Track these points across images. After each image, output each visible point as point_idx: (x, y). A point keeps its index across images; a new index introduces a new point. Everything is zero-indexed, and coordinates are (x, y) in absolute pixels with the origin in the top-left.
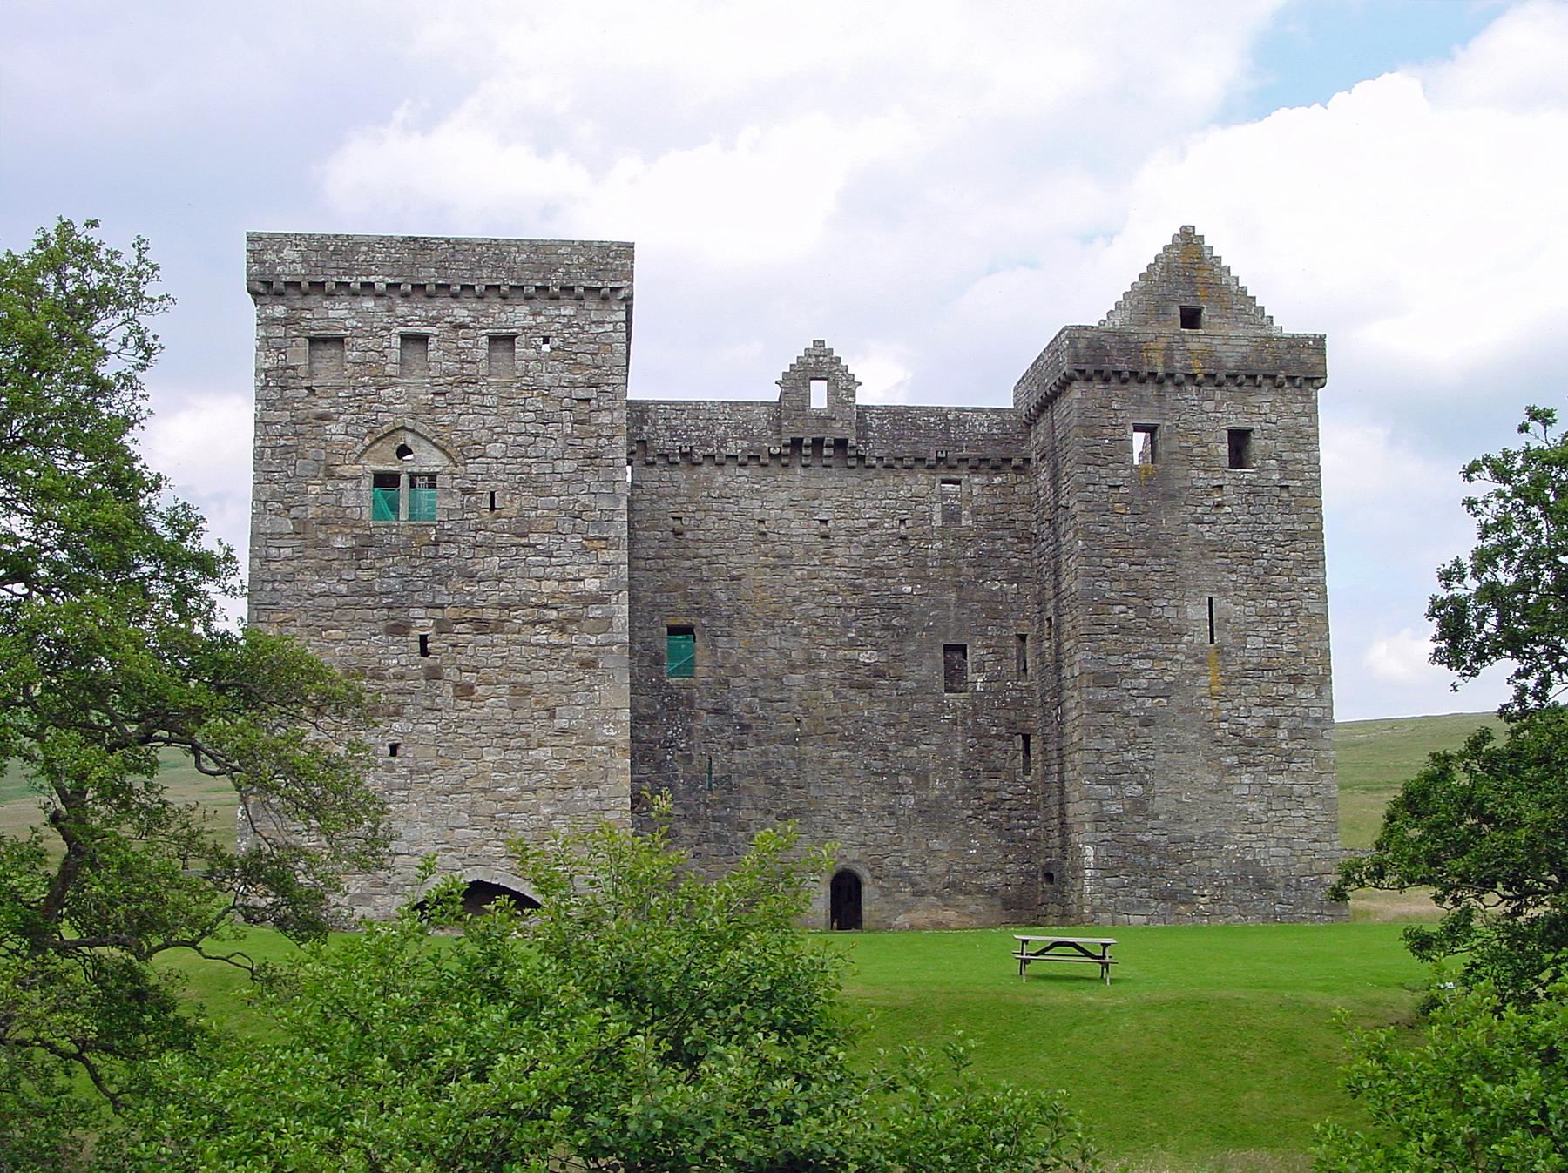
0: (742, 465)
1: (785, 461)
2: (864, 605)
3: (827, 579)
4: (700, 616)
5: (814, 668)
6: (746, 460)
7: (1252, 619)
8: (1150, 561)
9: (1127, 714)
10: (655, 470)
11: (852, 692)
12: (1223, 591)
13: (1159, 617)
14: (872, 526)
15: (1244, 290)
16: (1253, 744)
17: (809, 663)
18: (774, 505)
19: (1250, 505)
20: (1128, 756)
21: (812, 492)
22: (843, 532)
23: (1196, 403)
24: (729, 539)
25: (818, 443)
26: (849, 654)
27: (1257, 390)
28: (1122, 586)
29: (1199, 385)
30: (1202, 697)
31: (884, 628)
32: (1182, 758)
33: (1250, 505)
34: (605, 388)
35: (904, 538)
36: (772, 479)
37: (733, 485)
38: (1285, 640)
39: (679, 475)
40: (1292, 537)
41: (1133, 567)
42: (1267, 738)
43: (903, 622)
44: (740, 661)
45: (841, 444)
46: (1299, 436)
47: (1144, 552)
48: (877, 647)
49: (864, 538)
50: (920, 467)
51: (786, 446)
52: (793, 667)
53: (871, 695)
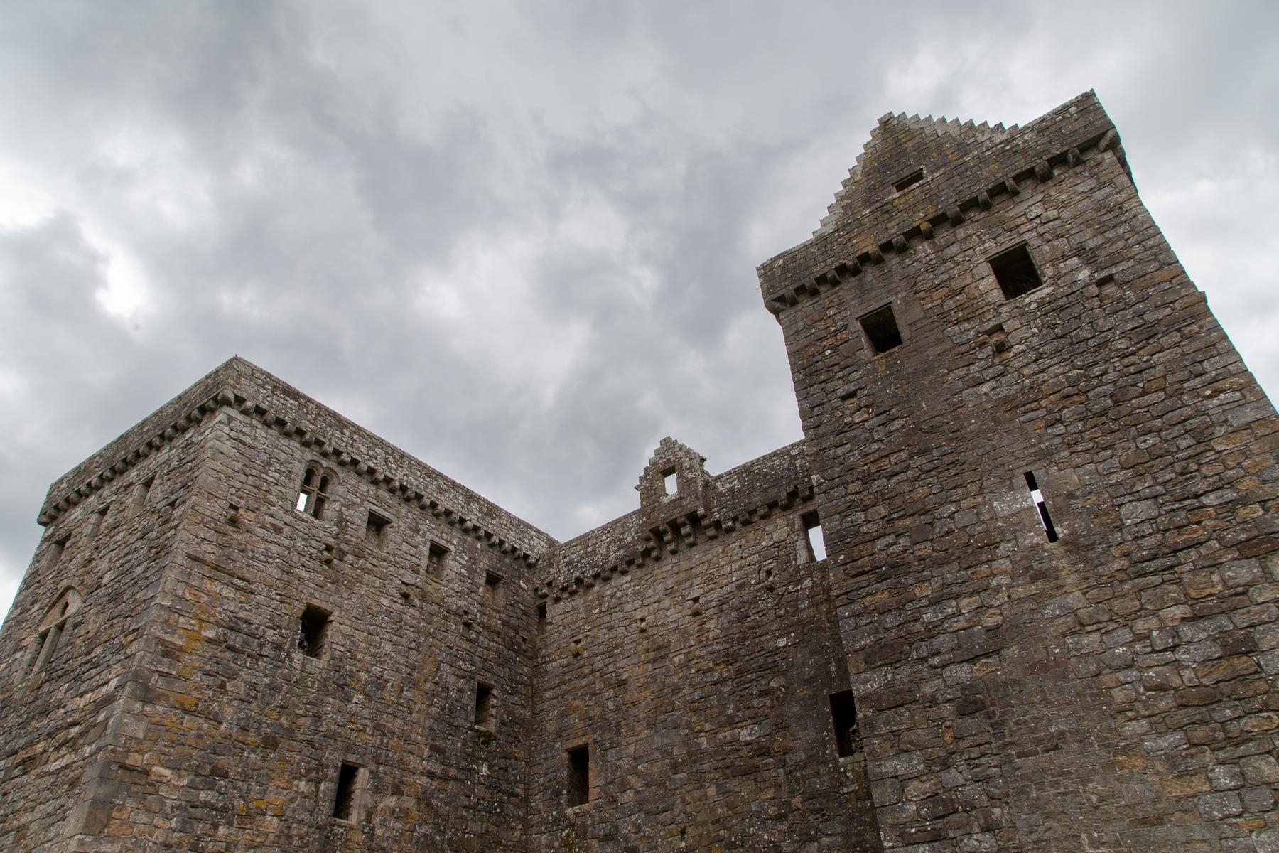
0: (624, 573)
1: (654, 554)
2: (740, 673)
3: (702, 657)
4: (594, 731)
5: (695, 762)
6: (624, 566)
8: (917, 462)
9: (933, 702)
10: (562, 604)
11: (736, 782)
12: (1045, 455)
13: (949, 533)
14: (739, 587)
16: (1212, 700)
17: (694, 756)
18: (652, 600)
19: (1053, 327)
21: (683, 575)
22: (713, 604)
23: (933, 256)
24: (617, 646)
25: (675, 526)
26: (726, 734)
27: (1017, 200)
29: (929, 236)
31: (764, 694)
32: (1057, 759)
33: (1053, 327)
34: (189, 484)
35: (770, 589)
37: (619, 594)
38: (1202, 487)
39: (578, 602)
40: (1148, 333)
41: (893, 481)
42: (1242, 678)
43: (782, 680)
44: (628, 772)
45: (694, 519)
47: (903, 455)
48: (756, 719)
49: (735, 602)
50: (777, 511)
51: (648, 539)
52: (676, 767)
53: (756, 780)
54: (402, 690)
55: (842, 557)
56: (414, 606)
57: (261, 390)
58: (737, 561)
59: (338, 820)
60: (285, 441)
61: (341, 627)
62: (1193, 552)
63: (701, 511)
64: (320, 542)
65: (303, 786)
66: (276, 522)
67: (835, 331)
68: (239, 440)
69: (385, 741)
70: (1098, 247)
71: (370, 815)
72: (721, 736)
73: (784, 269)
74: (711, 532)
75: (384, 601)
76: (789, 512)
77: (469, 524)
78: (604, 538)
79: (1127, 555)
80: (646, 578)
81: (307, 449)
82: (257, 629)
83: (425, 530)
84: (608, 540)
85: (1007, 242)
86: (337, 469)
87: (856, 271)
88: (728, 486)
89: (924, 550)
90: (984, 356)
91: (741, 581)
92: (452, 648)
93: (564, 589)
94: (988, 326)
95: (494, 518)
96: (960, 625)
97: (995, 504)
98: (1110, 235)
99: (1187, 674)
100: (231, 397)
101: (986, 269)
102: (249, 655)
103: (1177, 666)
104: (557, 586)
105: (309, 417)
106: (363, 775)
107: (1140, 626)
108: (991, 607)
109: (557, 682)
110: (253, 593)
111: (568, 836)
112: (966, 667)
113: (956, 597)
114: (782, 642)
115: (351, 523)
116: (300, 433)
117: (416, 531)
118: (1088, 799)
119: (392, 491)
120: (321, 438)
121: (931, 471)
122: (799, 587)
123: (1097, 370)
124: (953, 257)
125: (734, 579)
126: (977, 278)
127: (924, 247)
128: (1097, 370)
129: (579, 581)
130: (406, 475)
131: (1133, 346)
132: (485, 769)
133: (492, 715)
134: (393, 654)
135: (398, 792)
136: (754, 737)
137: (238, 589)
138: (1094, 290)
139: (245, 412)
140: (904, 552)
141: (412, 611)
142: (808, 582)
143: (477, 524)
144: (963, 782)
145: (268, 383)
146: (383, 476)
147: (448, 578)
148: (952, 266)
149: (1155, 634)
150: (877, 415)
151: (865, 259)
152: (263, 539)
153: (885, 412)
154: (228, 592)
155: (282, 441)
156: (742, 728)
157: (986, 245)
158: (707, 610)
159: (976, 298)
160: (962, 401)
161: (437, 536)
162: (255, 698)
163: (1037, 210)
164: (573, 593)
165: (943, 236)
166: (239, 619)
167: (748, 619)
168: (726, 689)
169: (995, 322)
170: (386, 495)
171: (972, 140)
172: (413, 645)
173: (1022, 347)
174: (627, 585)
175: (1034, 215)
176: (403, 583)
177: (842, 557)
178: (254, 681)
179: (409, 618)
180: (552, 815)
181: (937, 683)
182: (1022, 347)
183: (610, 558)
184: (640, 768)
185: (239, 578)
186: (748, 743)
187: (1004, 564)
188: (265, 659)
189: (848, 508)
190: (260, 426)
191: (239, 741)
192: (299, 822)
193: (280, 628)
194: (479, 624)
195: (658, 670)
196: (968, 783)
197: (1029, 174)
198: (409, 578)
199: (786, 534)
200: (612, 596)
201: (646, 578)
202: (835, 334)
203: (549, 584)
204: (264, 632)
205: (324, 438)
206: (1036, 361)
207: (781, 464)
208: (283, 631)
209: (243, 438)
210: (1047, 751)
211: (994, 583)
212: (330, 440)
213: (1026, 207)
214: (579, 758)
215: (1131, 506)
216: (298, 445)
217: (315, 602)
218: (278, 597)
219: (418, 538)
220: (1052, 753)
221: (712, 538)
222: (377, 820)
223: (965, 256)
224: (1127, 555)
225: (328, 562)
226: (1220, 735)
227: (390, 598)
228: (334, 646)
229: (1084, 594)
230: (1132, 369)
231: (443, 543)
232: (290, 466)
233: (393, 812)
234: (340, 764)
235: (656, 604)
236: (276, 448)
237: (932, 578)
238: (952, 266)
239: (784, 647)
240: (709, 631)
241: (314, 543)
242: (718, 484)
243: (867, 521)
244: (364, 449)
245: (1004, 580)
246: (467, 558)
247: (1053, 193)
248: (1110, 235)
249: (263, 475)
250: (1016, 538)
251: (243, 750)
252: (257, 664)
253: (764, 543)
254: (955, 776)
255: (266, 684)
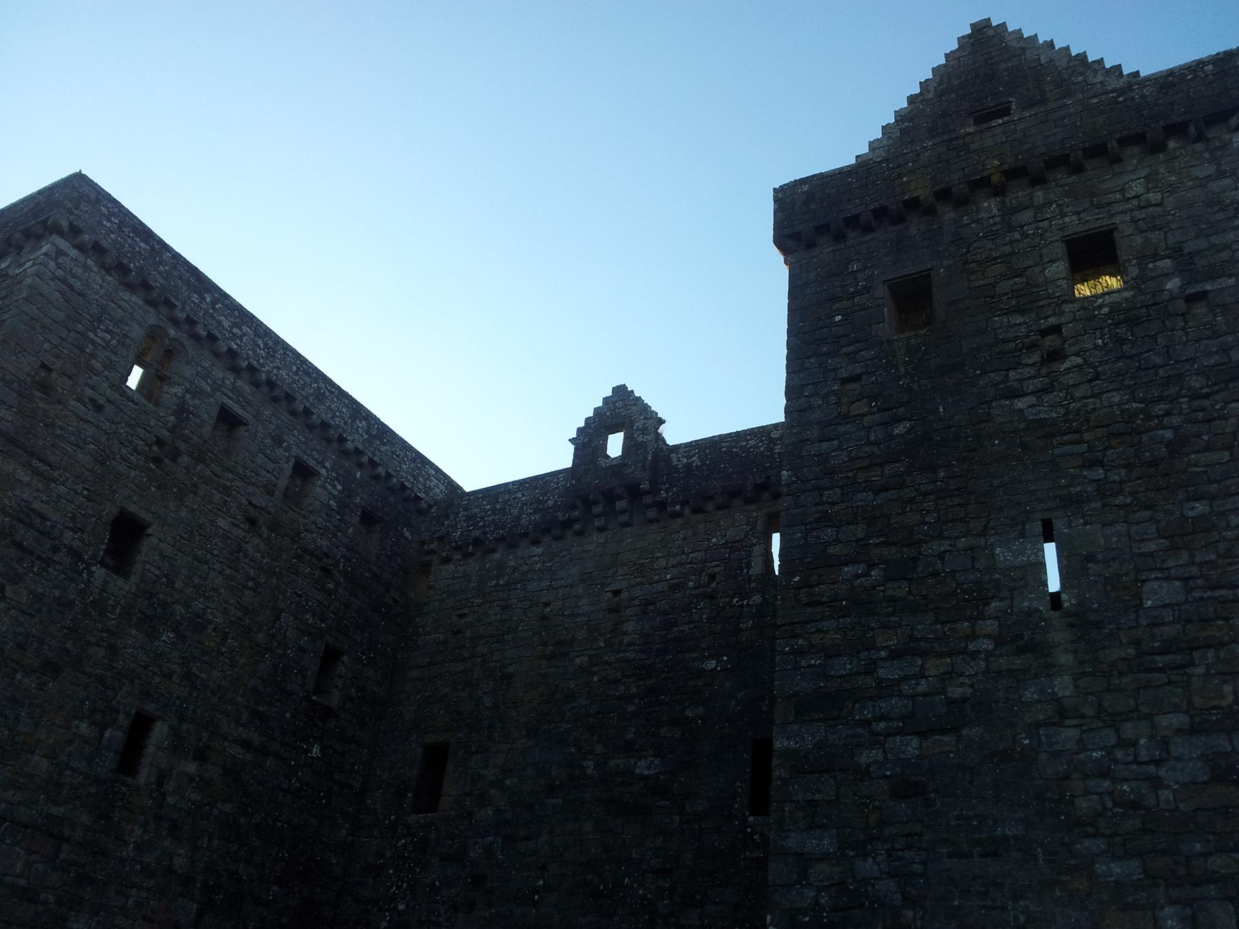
0: (536, 542)
1: (577, 527)
7: (1152, 546)
10: (451, 567)
14: (674, 588)
15: (1082, 57)
20: (868, 867)
23: (998, 219)
25: (610, 497)
26: (617, 762)
27: (1116, 168)
28: (860, 531)
29: (999, 192)
30: (1038, 725)
33: (1121, 341)
35: (710, 597)
36: (565, 553)
41: (882, 495)
45: (634, 492)
46: (1216, 208)
54: (226, 636)
55: (797, 579)
56: (260, 536)
57: (105, 223)
58: (677, 555)
59: (121, 777)
60: (125, 295)
61: (161, 544)
62: (1211, 654)
63: (645, 486)
64: (150, 432)
65: (84, 728)
66: (96, 397)
67: (853, 293)
68: (64, 281)
69: (195, 694)
70: (1198, 252)
71: (162, 777)
72: (612, 763)
73: (810, 196)
74: (652, 514)
75: (221, 523)
76: (753, 507)
77: (350, 445)
78: (519, 495)
79: (1137, 643)
80: (561, 555)
81: (152, 310)
82: (53, 527)
83: (292, 442)
84: (524, 498)
85: (1093, 220)
86: (188, 343)
87: (899, 219)
88: (685, 460)
89: (900, 590)
90: (1030, 361)
91: (677, 580)
92: (300, 596)
93: (458, 548)
94: (1044, 324)
95: (384, 444)
96: (920, 689)
97: (998, 551)
98: (1215, 240)
99: (1165, 794)
100: (65, 224)
101: (1060, 249)
102: (39, 558)
103: (1156, 783)
104: (450, 544)
105: (161, 268)
106: (160, 731)
107: (1129, 730)
108: (962, 674)
109: (426, 660)
110: (54, 482)
111: (404, 846)
112: (915, 741)
113: (924, 654)
114: (712, 664)
115: (195, 416)
116: (145, 286)
117: (279, 441)
118: (1016, 918)
119: (256, 384)
120: (173, 300)
121: (931, 494)
122: (745, 602)
123: (1159, 409)
124: (1022, 226)
125: (669, 576)
126: (1046, 260)
127: (989, 205)
128: (1159, 409)
129: (477, 542)
130: (278, 369)
131: (1208, 387)
132: (316, 751)
133: (337, 687)
134: (222, 590)
135: (201, 755)
136: (652, 772)
137: (36, 472)
138: (1181, 305)
139: (80, 247)
140: (874, 587)
141: (256, 540)
142: (757, 599)
143: (361, 447)
144: (878, 874)
145: (114, 215)
146: (246, 363)
147: (311, 508)
148: (1019, 237)
149: (1142, 741)
150: (879, 411)
151: (913, 204)
152: (77, 416)
153: (891, 409)
154: (24, 475)
155: (121, 294)
156: (640, 758)
157: (1067, 219)
158: (627, 608)
159: (1037, 286)
160: (989, 414)
161: (305, 453)
162: (39, 611)
163: (1137, 188)
164: (467, 555)
165: (1018, 194)
166: (31, 509)
167: (676, 629)
168: (631, 708)
169: (1053, 320)
170: (247, 388)
171: (1080, 78)
172: (250, 584)
173: (1079, 360)
174: (537, 559)
175: (1132, 194)
176: (250, 503)
177: (797, 579)
178: (40, 590)
179: (250, 549)
180: (390, 819)
181: (876, 754)
182: (1079, 360)
183: (522, 522)
184: (507, 782)
185: (41, 460)
186: (644, 778)
187: (991, 626)
188: (57, 567)
189: (818, 521)
190: (95, 269)
191: (12, 660)
192: (73, 769)
193: (83, 532)
194: (340, 573)
195: (553, 670)
196: (884, 876)
197: (1138, 139)
198: (260, 500)
199: (743, 535)
200: (515, 570)
201: (561, 555)
202: (852, 296)
203: (441, 539)
204: (62, 533)
205: (177, 299)
206: (1090, 381)
207: (755, 447)
208: (86, 536)
209: (72, 281)
210: (985, 855)
211: (971, 647)
212: (184, 303)
213: (1126, 181)
214: (437, 757)
215: (1156, 585)
216: (140, 303)
217: (132, 508)
218: (86, 493)
219: (280, 452)
220: (989, 860)
221: (651, 521)
222: (170, 786)
223: (1037, 228)
224: (1137, 643)
225: (157, 460)
226: (1181, 871)
227: (229, 520)
228: (148, 566)
229: (1075, 680)
230: (1200, 415)
231: (312, 463)
232: (127, 328)
233: (192, 780)
234: (133, 712)
235: (568, 589)
236: (113, 302)
237: (900, 626)
238: (1019, 237)
239: (712, 670)
240: (626, 633)
241: (141, 431)
242: (673, 455)
243: (837, 541)
244: (226, 324)
245: (987, 645)
246: (339, 487)
247: (1162, 171)
248: (1215, 240)
249: (91, 335)
250: (1012, 598)
251: (16, 671)
252: (47, 571)
253: (714, 540)
254: (868, 867)
255: (54, 597)
